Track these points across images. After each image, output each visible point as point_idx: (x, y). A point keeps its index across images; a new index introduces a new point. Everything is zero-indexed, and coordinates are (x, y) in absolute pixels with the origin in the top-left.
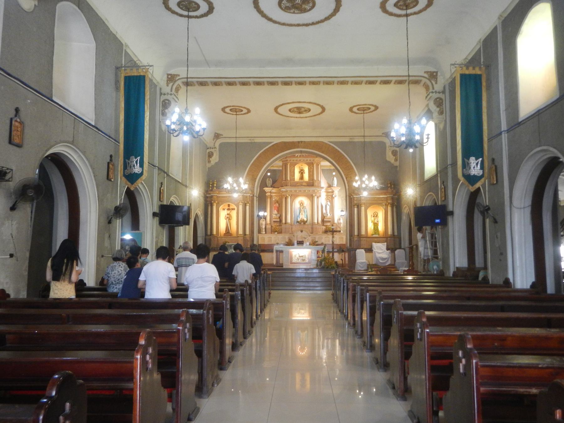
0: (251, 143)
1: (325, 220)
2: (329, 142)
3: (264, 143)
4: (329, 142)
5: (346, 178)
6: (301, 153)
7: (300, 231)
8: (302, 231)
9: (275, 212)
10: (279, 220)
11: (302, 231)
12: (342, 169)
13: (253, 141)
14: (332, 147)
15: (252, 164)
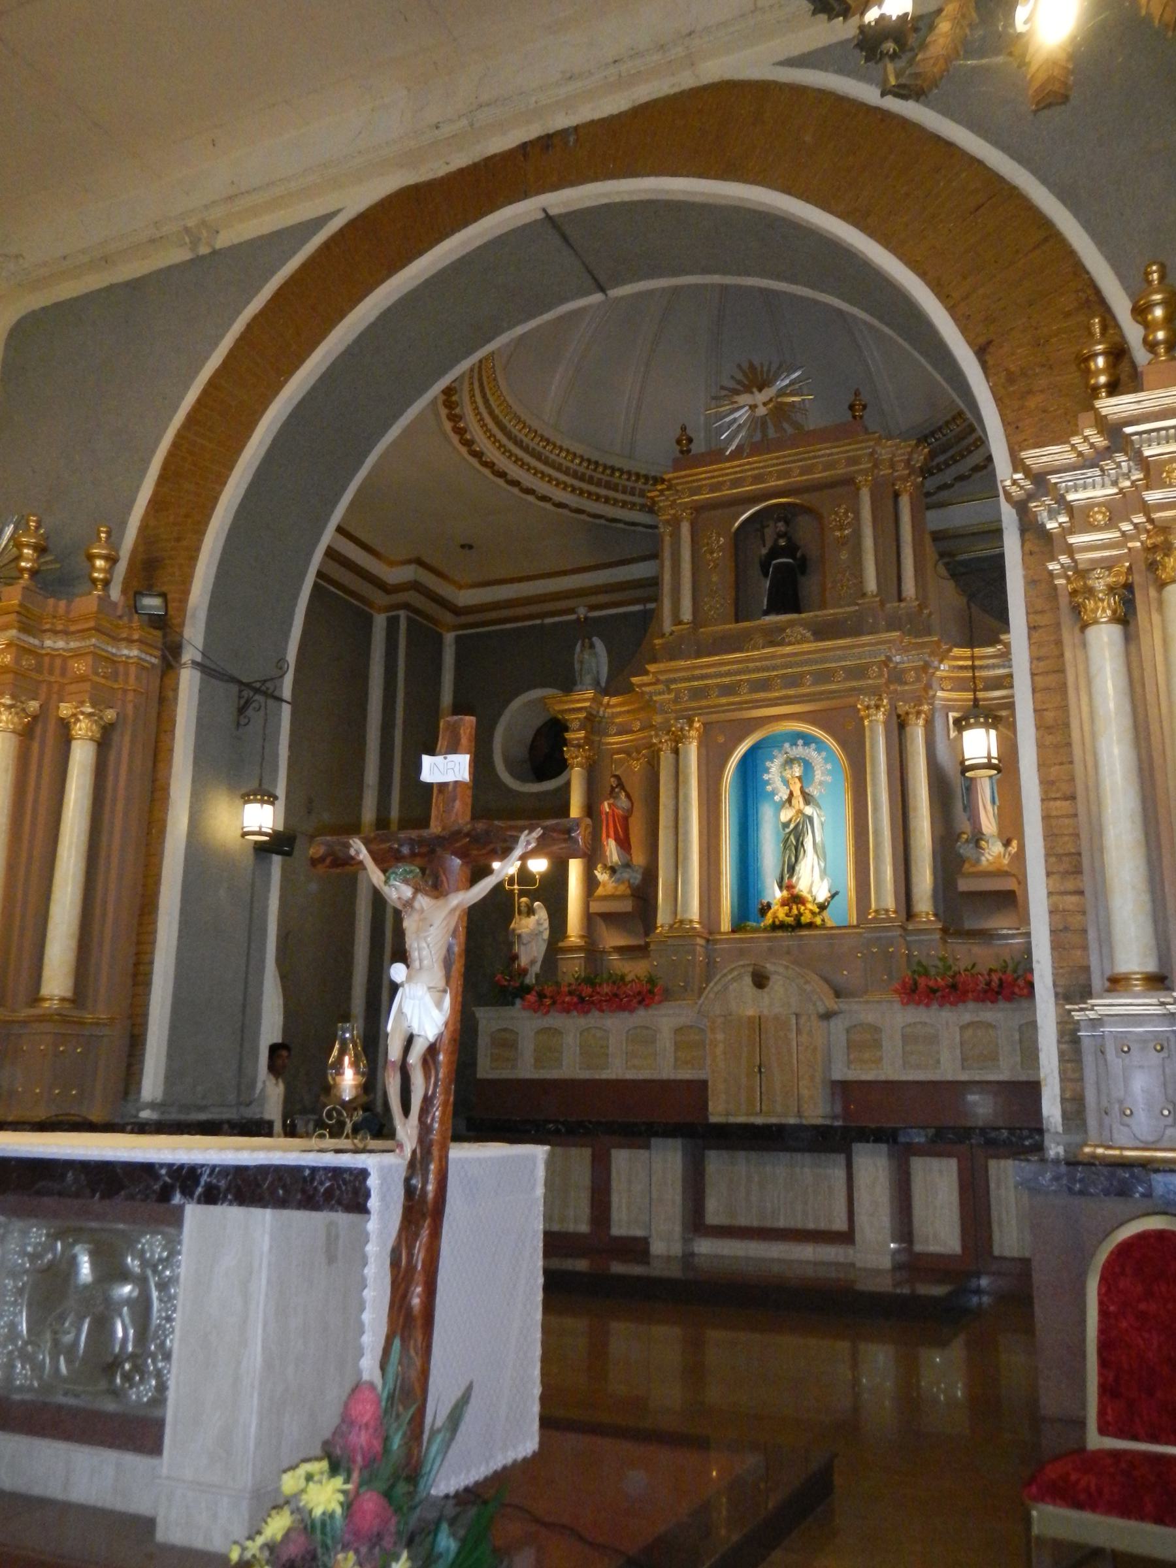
0: (197, 261)
1: (964, 885)
2: (791, 62)
3: (278, 235)
4: (791, 62)
5: (981, 353)
6: (603, 290)
7: (748, 980)
8: (760, 980)
9: (612, 851)
10: (626, 906)
11: (760, 980)
12: (922, 275)
13: (204, 250)
14: (823, 95)
15: (191, 419)
